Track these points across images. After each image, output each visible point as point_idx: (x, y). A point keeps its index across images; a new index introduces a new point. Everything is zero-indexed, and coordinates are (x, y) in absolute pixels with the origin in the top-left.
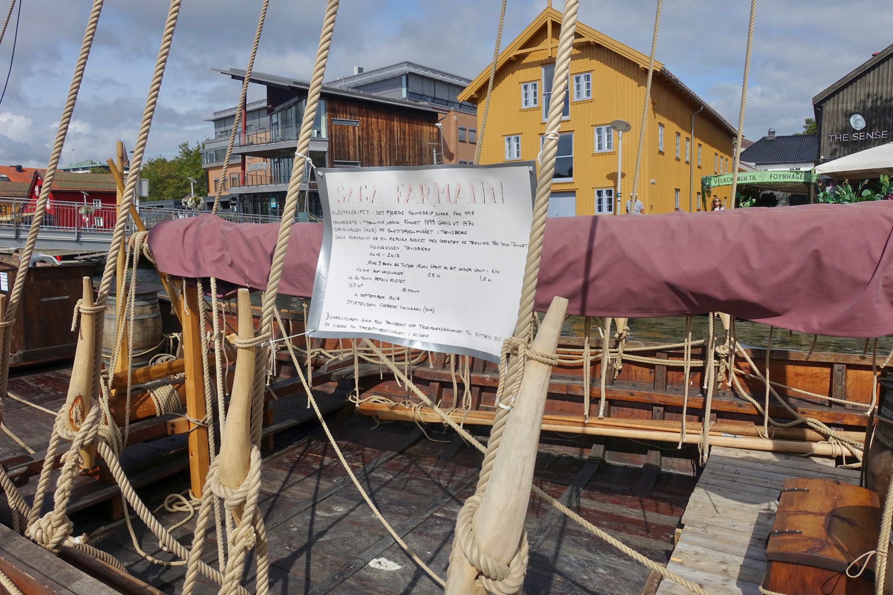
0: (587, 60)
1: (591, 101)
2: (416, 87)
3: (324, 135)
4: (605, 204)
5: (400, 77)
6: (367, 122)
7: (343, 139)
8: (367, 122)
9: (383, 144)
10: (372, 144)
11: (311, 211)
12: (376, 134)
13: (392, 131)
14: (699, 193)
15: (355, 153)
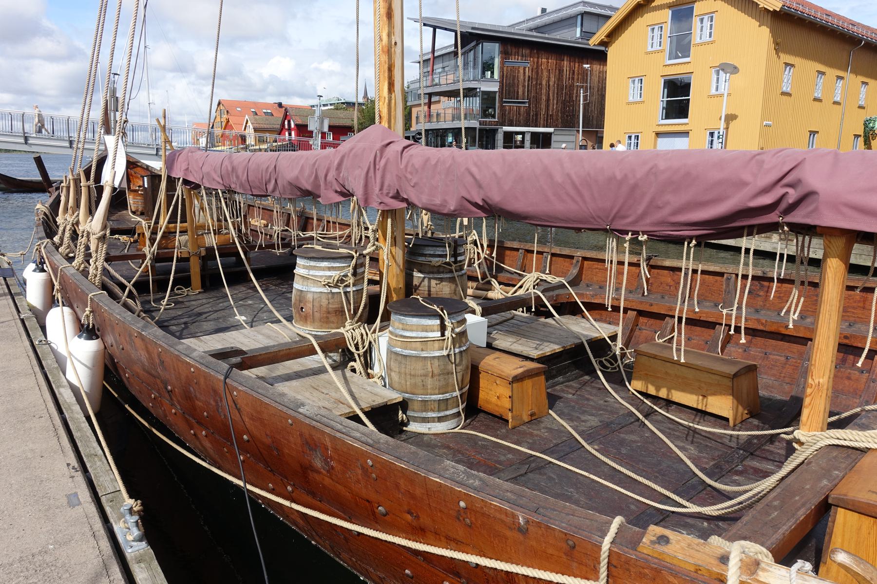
3: (496, 76)
5: (575, 17)
6: (538, 62)
7: (513, 80)
8: (538, 62)
9: (551, 83)
10: (541, 84)
12: (545, 74)
13: (561, 71)
15: (524, 93)
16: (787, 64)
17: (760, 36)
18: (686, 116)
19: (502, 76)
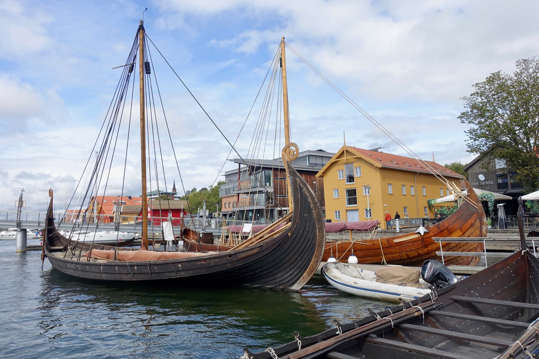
0: (359, 163)
2: (313, 161)
3: (272, 185)
4: (369, 215)
5: (306, 156)
14: (425, 207)
17: (377, 175)
18: (356, 203)
19: (275, 185)
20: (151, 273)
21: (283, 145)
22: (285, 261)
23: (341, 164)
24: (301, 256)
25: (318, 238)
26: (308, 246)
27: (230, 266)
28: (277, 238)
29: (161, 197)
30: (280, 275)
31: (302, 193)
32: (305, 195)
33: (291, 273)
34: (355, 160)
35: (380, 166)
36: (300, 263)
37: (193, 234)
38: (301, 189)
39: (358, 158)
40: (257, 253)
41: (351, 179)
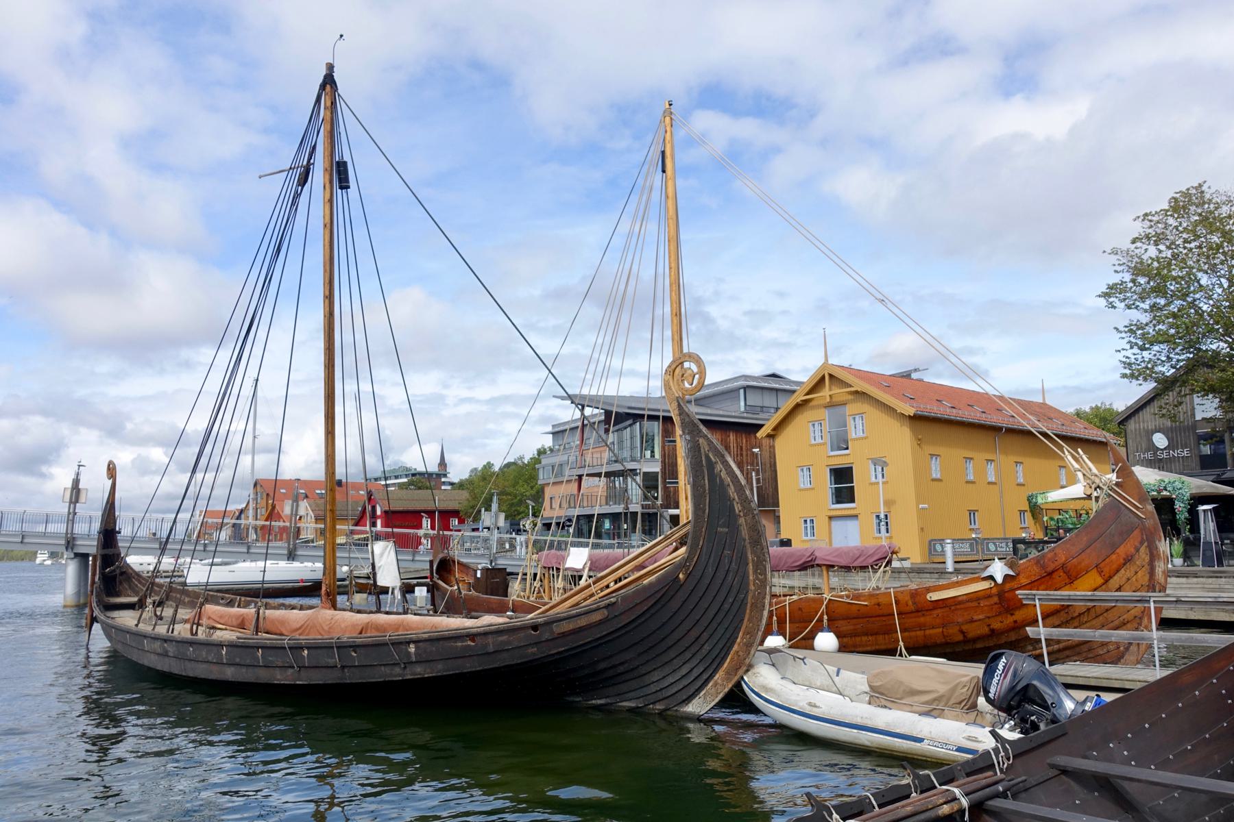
0: (859, 404)
1: (866, 438)
2: (754, 399)
3: (657, 455)
4: (883, 528)
5: (737, 390)
11: (644, 532)
14: (1022, 512)
16: (932, 455)
17: (902, 436)
18: (853, 501)
19: (663, 456)
20: (343, 667)
21: (668, 359)
22: (669, 642)
23: (818, 407)
24: (710, 630)
25: (752, 587)
26: (726, 606)
27: (534, 654)
28: (650, 584)
29: (410, 483)
30: (656, 676)
31: (713, 476)
32: (722, 480)
33: (684, 671)
34: (850, 397)
35: (911, 411)
36: (707, 647)
37: (461, 571)
38: (711, 466)
39: (857, 392)
40: (601, 622)
41: (842, 443)
